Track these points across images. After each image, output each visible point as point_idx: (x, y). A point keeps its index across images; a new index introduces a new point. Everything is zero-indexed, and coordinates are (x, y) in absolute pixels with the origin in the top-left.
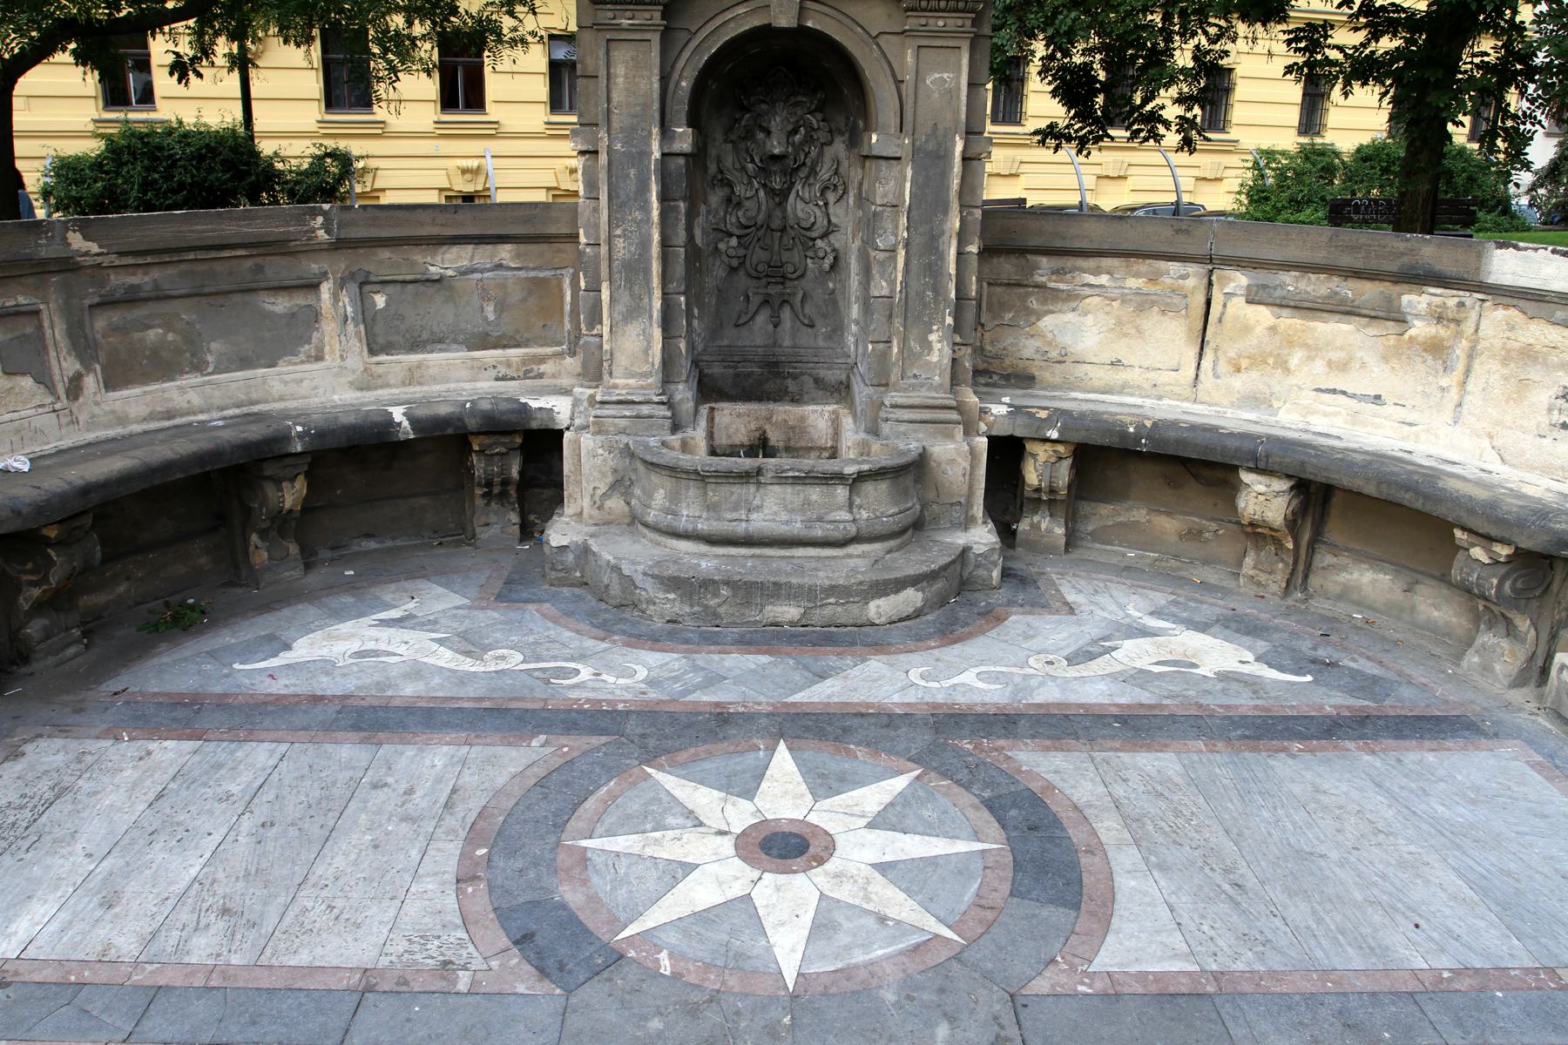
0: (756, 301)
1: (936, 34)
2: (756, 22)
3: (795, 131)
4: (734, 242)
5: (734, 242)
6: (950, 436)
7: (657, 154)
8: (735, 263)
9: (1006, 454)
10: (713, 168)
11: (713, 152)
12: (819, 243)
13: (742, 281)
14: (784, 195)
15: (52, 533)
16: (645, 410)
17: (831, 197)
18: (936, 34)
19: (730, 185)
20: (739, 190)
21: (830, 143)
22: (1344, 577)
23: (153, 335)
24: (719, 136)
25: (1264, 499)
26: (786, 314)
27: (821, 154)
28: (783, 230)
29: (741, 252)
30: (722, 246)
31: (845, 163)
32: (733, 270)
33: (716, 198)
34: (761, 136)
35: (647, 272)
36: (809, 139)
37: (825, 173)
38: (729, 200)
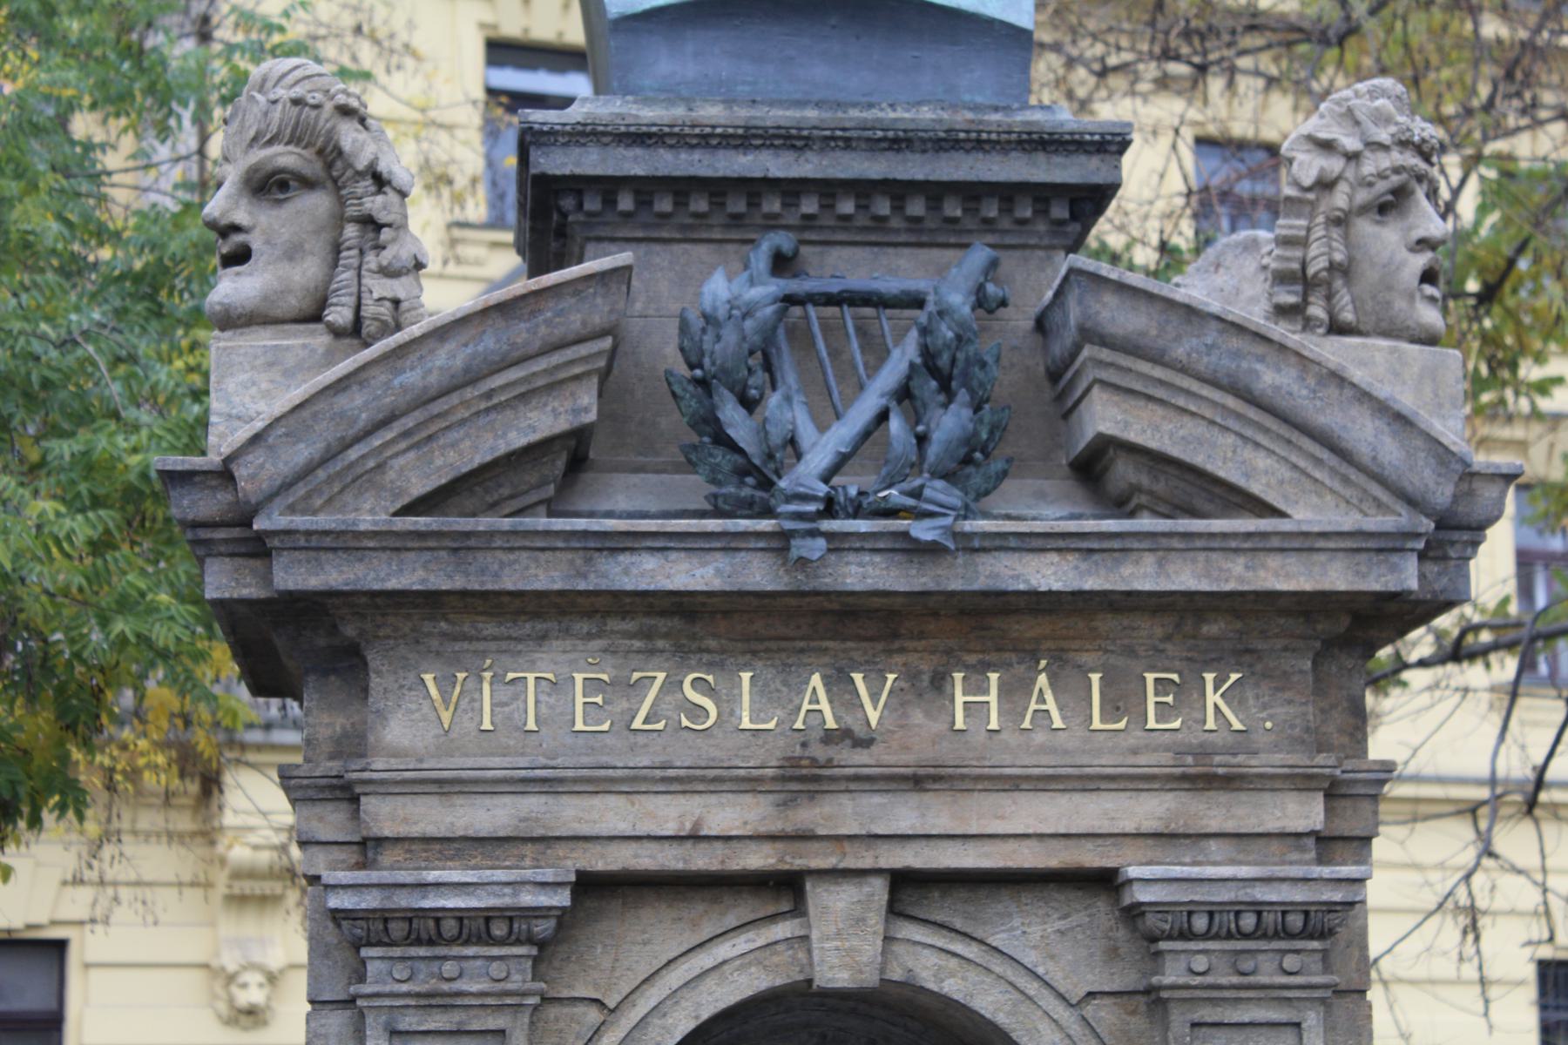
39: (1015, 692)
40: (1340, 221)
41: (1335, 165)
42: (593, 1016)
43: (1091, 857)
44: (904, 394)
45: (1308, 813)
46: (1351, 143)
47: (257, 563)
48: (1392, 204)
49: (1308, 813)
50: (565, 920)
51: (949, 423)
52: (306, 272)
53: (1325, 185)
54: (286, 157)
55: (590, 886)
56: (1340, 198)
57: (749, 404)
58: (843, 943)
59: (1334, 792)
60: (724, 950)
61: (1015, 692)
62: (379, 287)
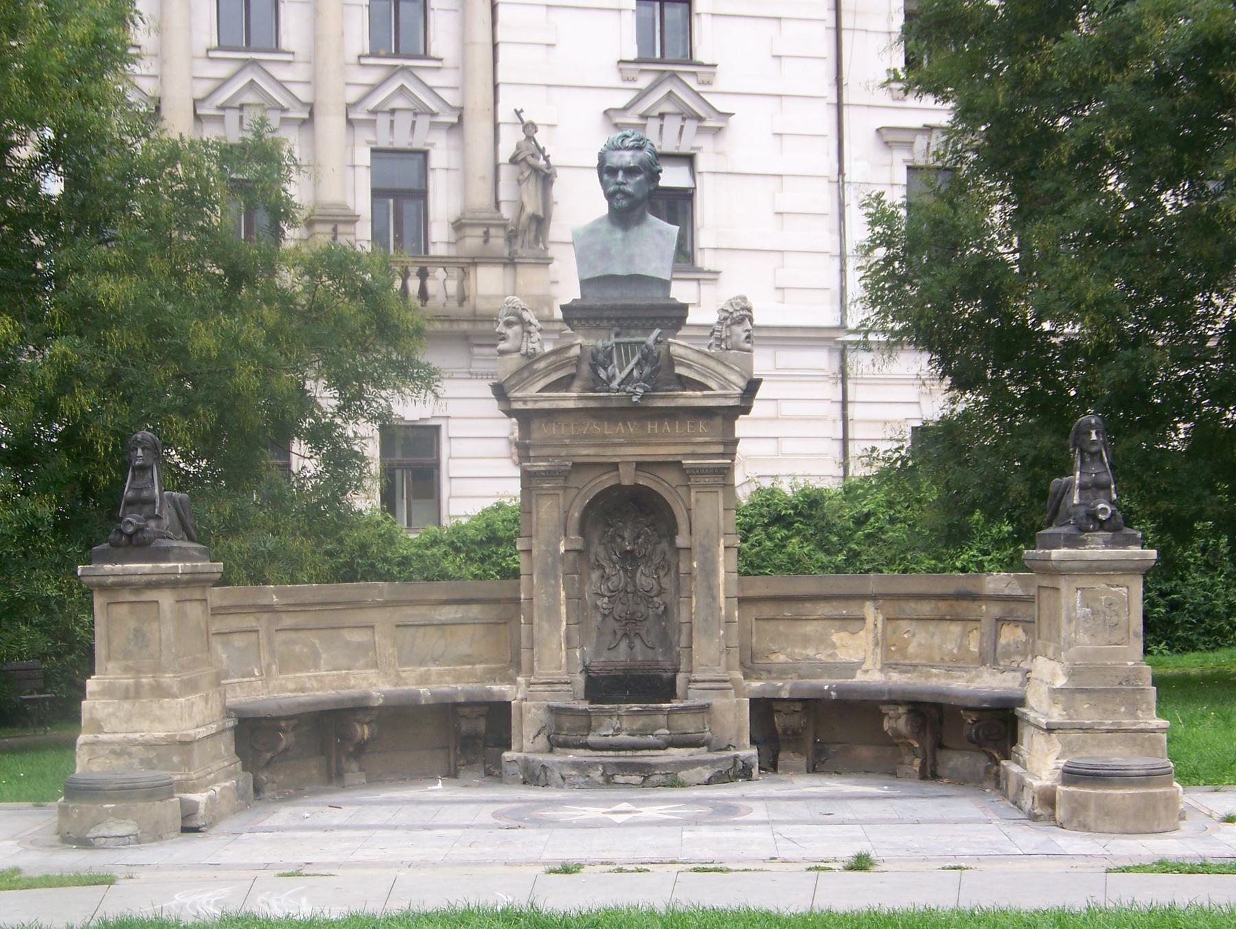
0: (620, 633)
1: (705, 486)
2: (613, 482)
3: (639, 537)
4: (606, 600)
5: (606, 600)
6: (726, 696)
7: (562, 550)
8: (606, 612)
9: (763, 708)
10: (593, 559)
11: (593, 550)
12: (655, 599)
13: (610, 621)
14: (634, 572)
15: (283, 724)
16: (558, 687)
17: (662, 573)
18: (705, 486)
19: (603, 568)
20: (607, 570)
21: (659, 543)
22: (951, 764)
23: (297, 648)
24: (596, 541)
25: (897, 722)
26: (637, 642)
27: (654, 550)
28: (634, 593)
29: (610, 606)
30: (599, 603)
31: (668, 554)
32: (605, 616)
33: (595, 576)
34: (619, 540)
35: (558, 613)
36: (647, 541)
37: (657, 559)
38: (603, 577)
39: (661, 425)
40: (728, 326)
41: (726, 314)
42: (576, 491)
43: (679, 458)
44: (637, 364)
45: (720, 449)
46: (731, 310)
47: (509, 270)
48: (740, 321)
49: (720, 449)
50: (570, 471)
51: (647, 370)
52: (517, 343)
53: (725, 319)
54: (512, 318)
55: (574, 464)
56: (729, 322)
57: (606, 369)
58: (627, 478)
59: (725, 444)
60: (605, 477)
61: (661, 425)
62: (531, 345)
